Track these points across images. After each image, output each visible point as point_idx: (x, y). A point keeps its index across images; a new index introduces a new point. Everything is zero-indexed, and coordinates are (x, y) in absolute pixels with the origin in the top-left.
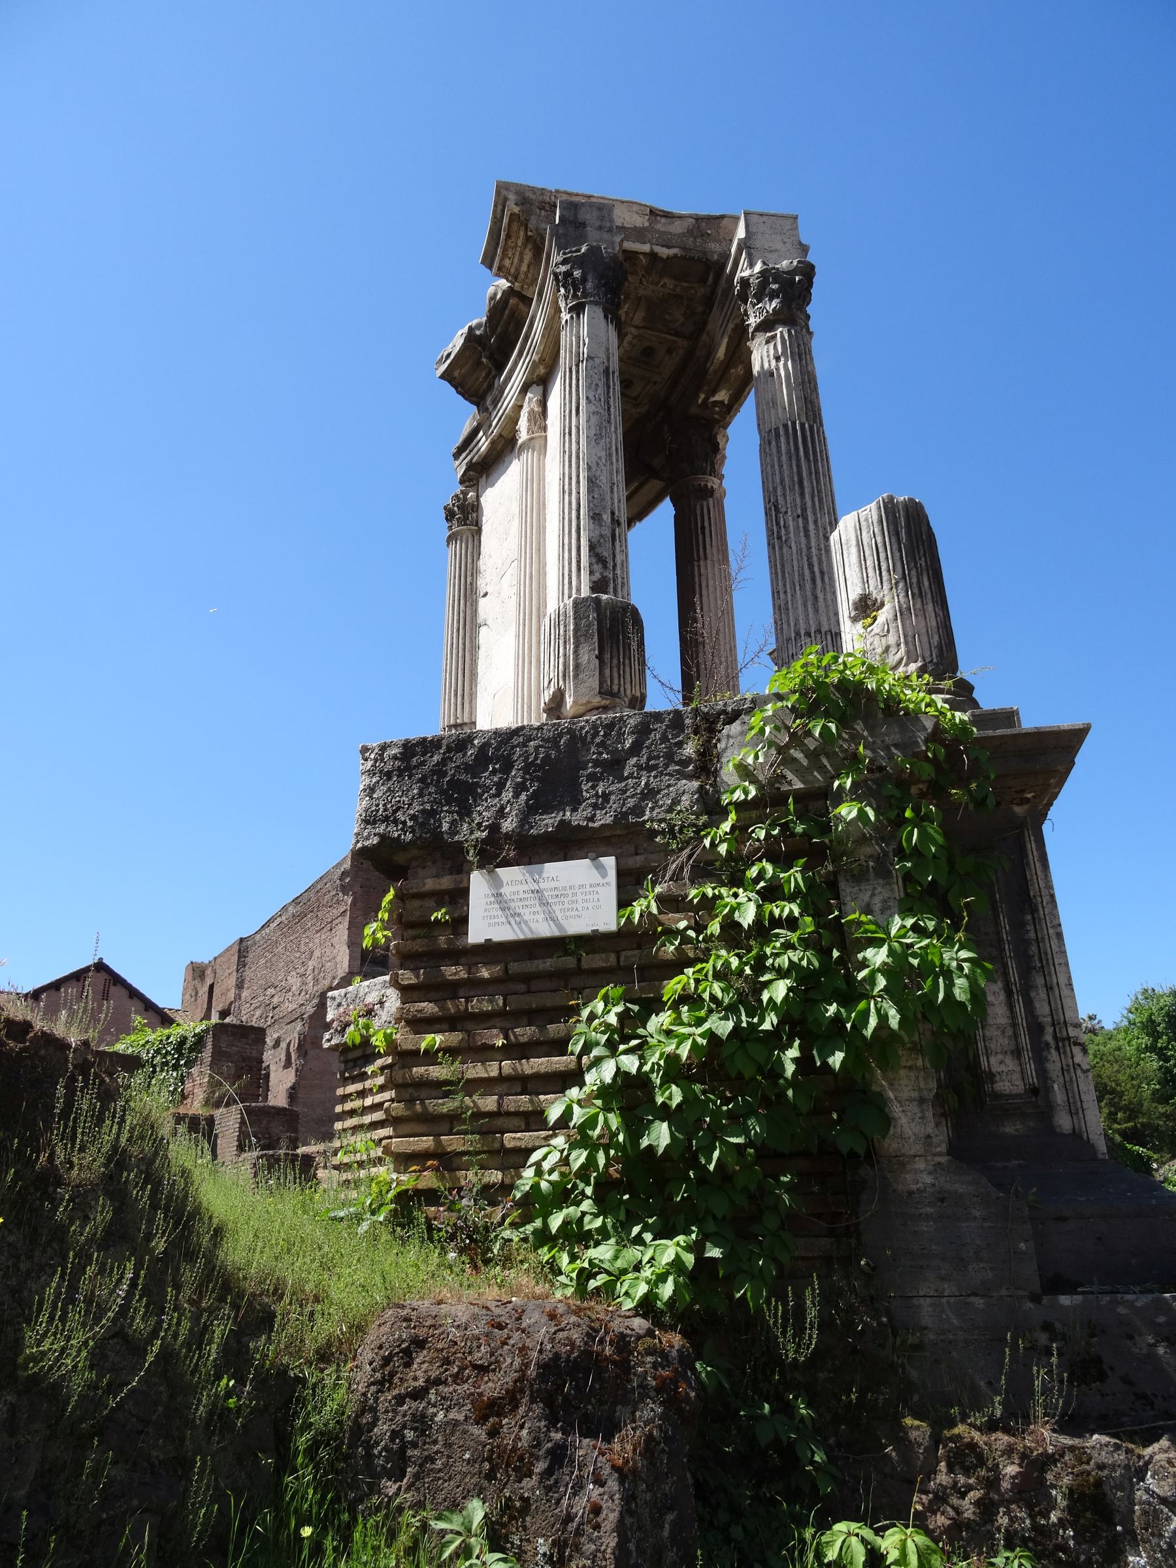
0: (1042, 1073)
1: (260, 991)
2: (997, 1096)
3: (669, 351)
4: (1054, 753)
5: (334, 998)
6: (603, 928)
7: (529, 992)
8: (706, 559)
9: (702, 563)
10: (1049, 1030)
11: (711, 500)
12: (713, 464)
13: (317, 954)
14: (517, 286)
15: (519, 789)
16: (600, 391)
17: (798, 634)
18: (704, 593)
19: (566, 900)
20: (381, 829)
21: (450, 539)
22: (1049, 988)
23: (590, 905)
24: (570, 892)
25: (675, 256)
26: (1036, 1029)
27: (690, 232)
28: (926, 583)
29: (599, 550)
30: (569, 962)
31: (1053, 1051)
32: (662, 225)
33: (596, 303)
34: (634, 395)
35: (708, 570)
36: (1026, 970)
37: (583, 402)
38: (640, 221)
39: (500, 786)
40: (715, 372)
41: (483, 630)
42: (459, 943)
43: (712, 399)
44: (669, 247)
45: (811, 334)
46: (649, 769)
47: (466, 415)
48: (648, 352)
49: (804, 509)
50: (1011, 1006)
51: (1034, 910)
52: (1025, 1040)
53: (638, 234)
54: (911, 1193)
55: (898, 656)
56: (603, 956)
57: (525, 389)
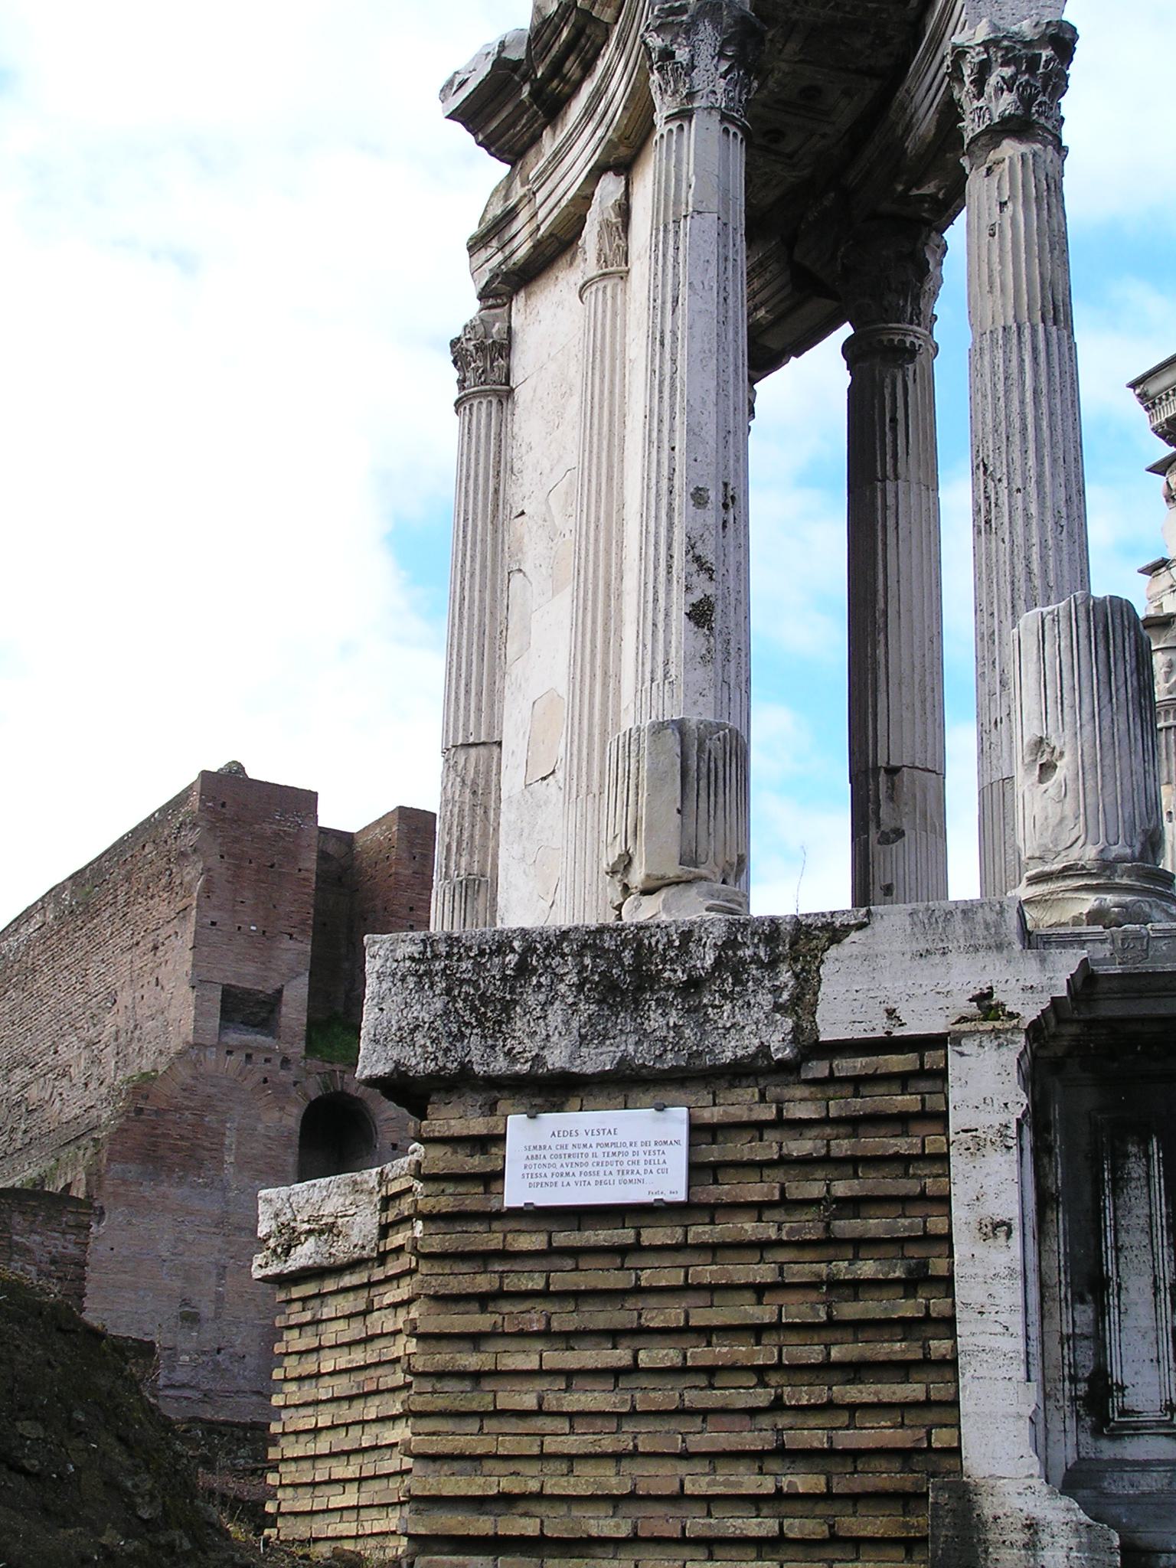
2: (1123, 1412)
5: (269, 1201)
6: (669, 1198)
7: (576, 1269)
8: (897, 478)
9: (890, 485)
11: (910, 366)
13: (124, 998)
19: (625, 1159)
20: (394, 1053)
21: (458, 404)
23: (654, 1168)
24: (630, 1150)
29: (698, 551)
30: (626, 1236)
34: (789, 150)
35: (904, 496)
37: (684, 291)
42: (493, 1205)
43: (915, 192)
54: (996, 1518)
56: (669, 1231)
57: (595, 175)
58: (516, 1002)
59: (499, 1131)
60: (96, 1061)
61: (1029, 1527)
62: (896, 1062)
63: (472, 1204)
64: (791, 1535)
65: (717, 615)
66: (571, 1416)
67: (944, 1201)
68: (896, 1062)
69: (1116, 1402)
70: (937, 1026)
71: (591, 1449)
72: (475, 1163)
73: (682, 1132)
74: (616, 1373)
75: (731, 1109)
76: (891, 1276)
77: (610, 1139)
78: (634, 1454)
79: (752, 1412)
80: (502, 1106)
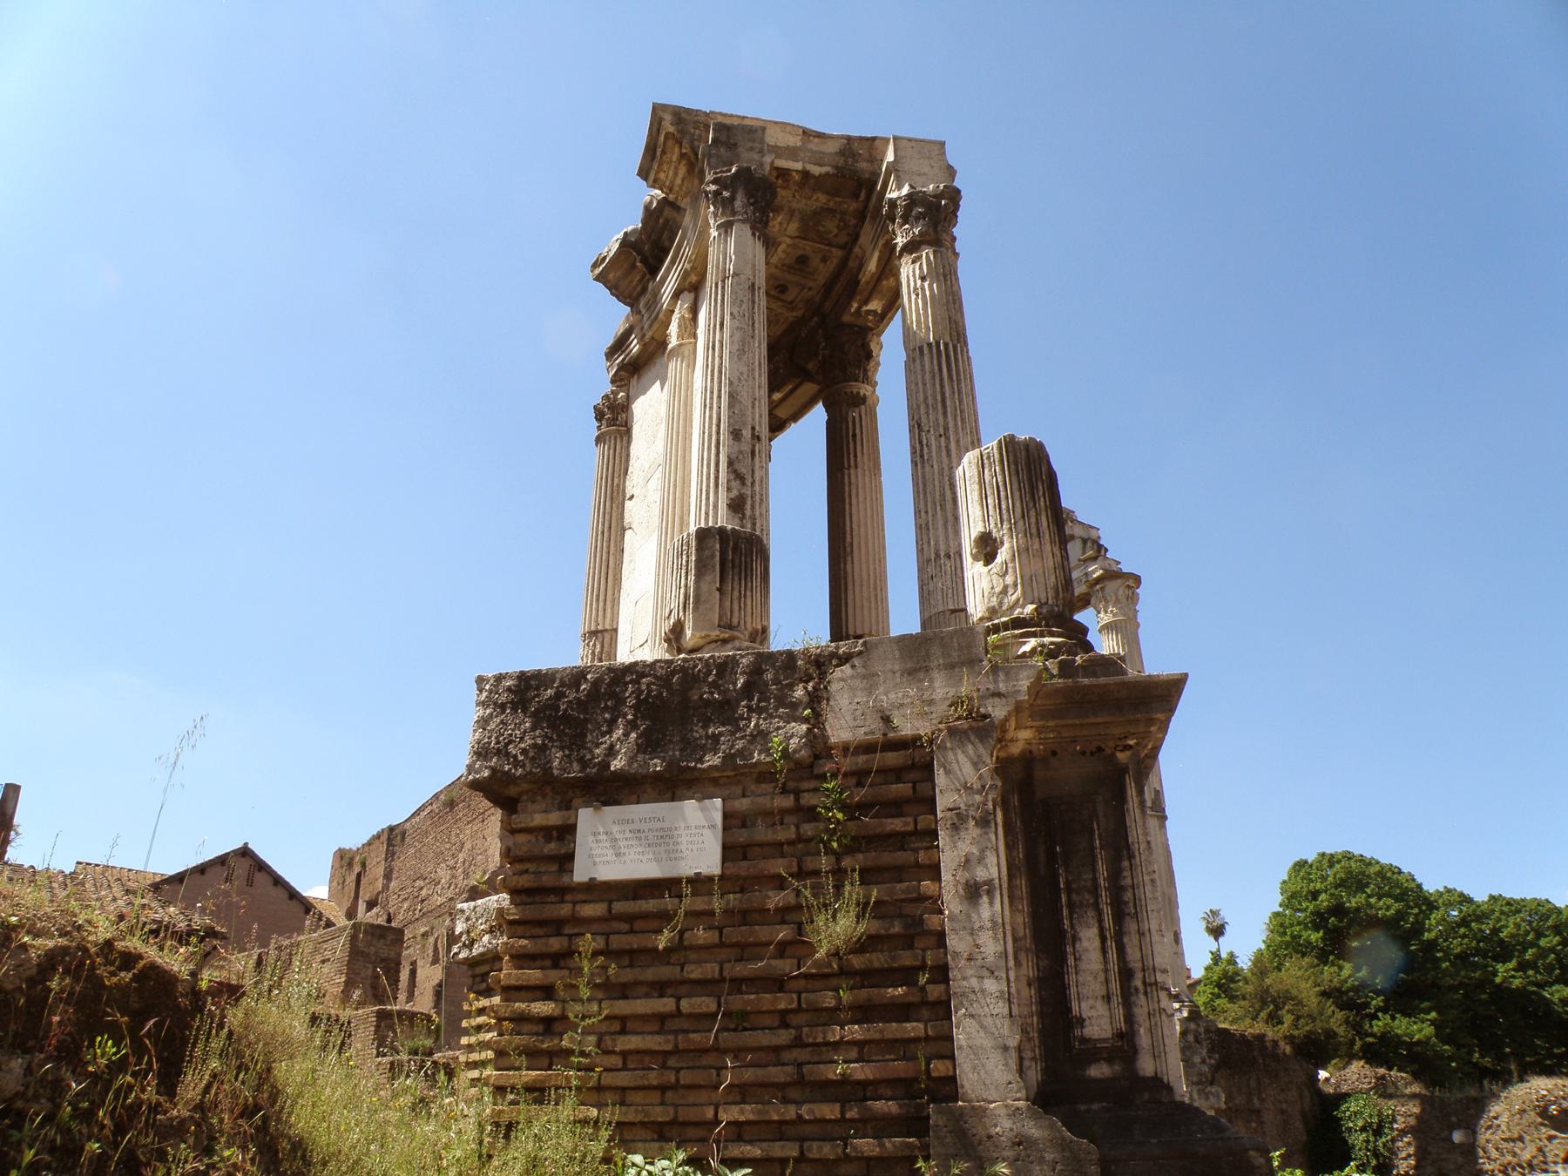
0: (1130, 1018)
1: (409, 882)
2: (1084, 1040)
3: (824, 260)
4: (1162, 696)
5: (462, 911)
7: (632, 931)
10: (1139, 975)
12: (866, 371)
13: (468, 845)
14: (671, 197)
15: (632, 725)
16: (744, 306)
17: (937, 555)
18: (854, 501)
21: (598, 440)
22: (1141, 934)
25: (827, 174)
26: (1126, 974)
27: (841, 153)
28: (1045, 524)
29: (737, 466)
31: (1142, 997)
32: (814, 145)
33: (743, 221)
35: (858, 478)
36: (1119, 917)
37: (727, 318)
38: (795, 141)
39: (612, 724)
40: (867, 283)
41: (628, 533)
42: (565, 879)
44: (821, 165)
45: (956, 255)
46: (759, 711)
47: (616, 315)
48: (803, 260)
49: (946, 429)
50: (1104, 951)
51: (1131, 857)
52: (1115, 986)
53: (792, 153)
55: (1014, 597)
57: (677, 295)
58: (586, 721)
59: (571, 821)
60: (454, 877)
61: (1019, 1144)
62: (892, 758)
63: (547, 881)
64: (811, 1156)
65: (748, 506)
66: (625, 1054)
67: (934, 871)
68: (892, 758)
69: (1077, 1032)
70: (923, 729)
71: (640, 1083)
72: (552, 848)
73: (718, 818)
74: (662, 1018)
75: (760, 800)
76: (892, 931)
77: (659, 825)
78: (676, 1087)
79: (776, 1049)
80: (575, 802)
